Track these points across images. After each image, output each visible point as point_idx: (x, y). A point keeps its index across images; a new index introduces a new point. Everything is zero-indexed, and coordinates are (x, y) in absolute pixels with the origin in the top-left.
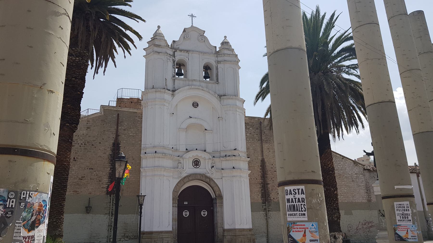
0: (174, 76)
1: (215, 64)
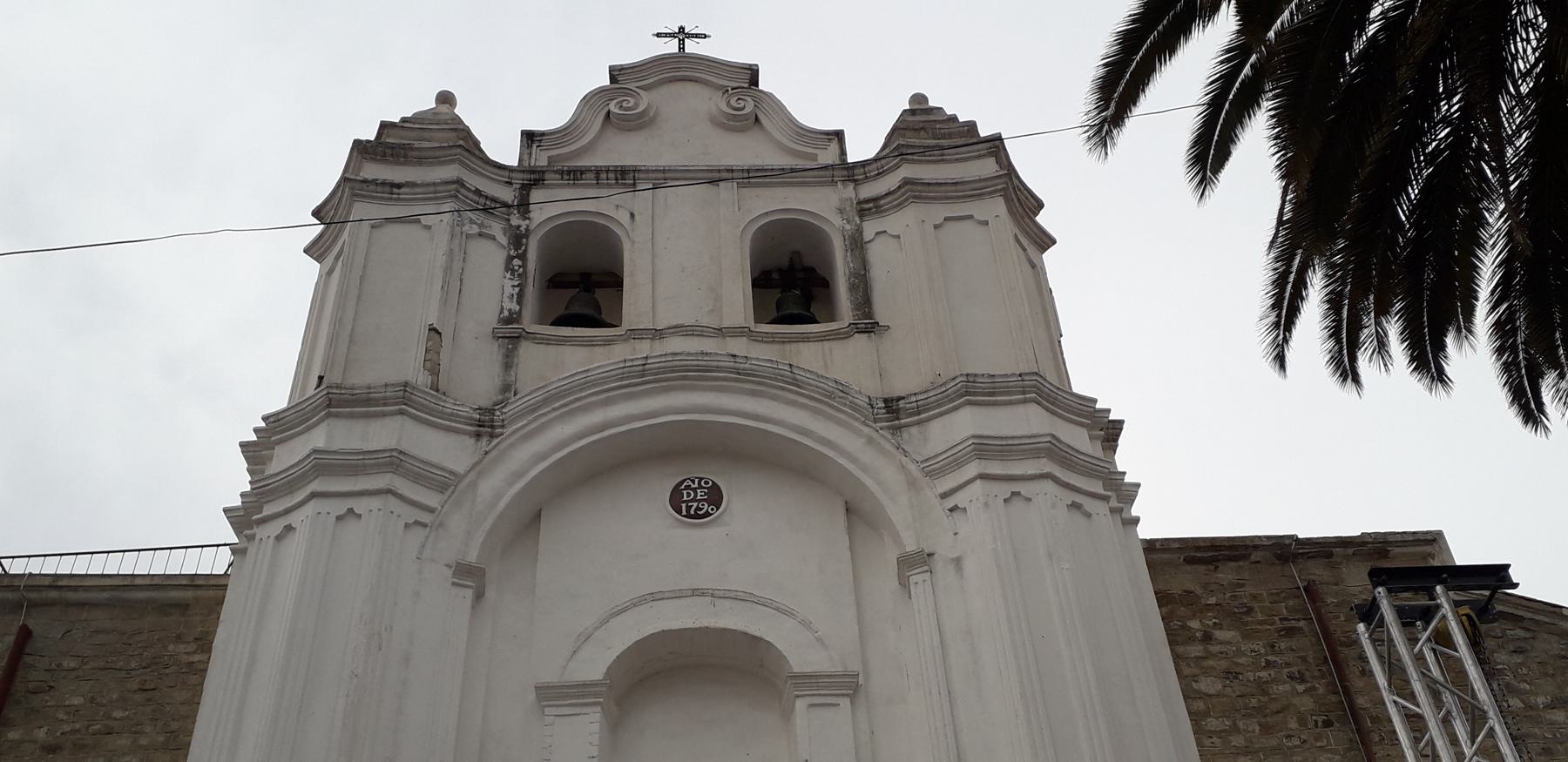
1: (837, 221)
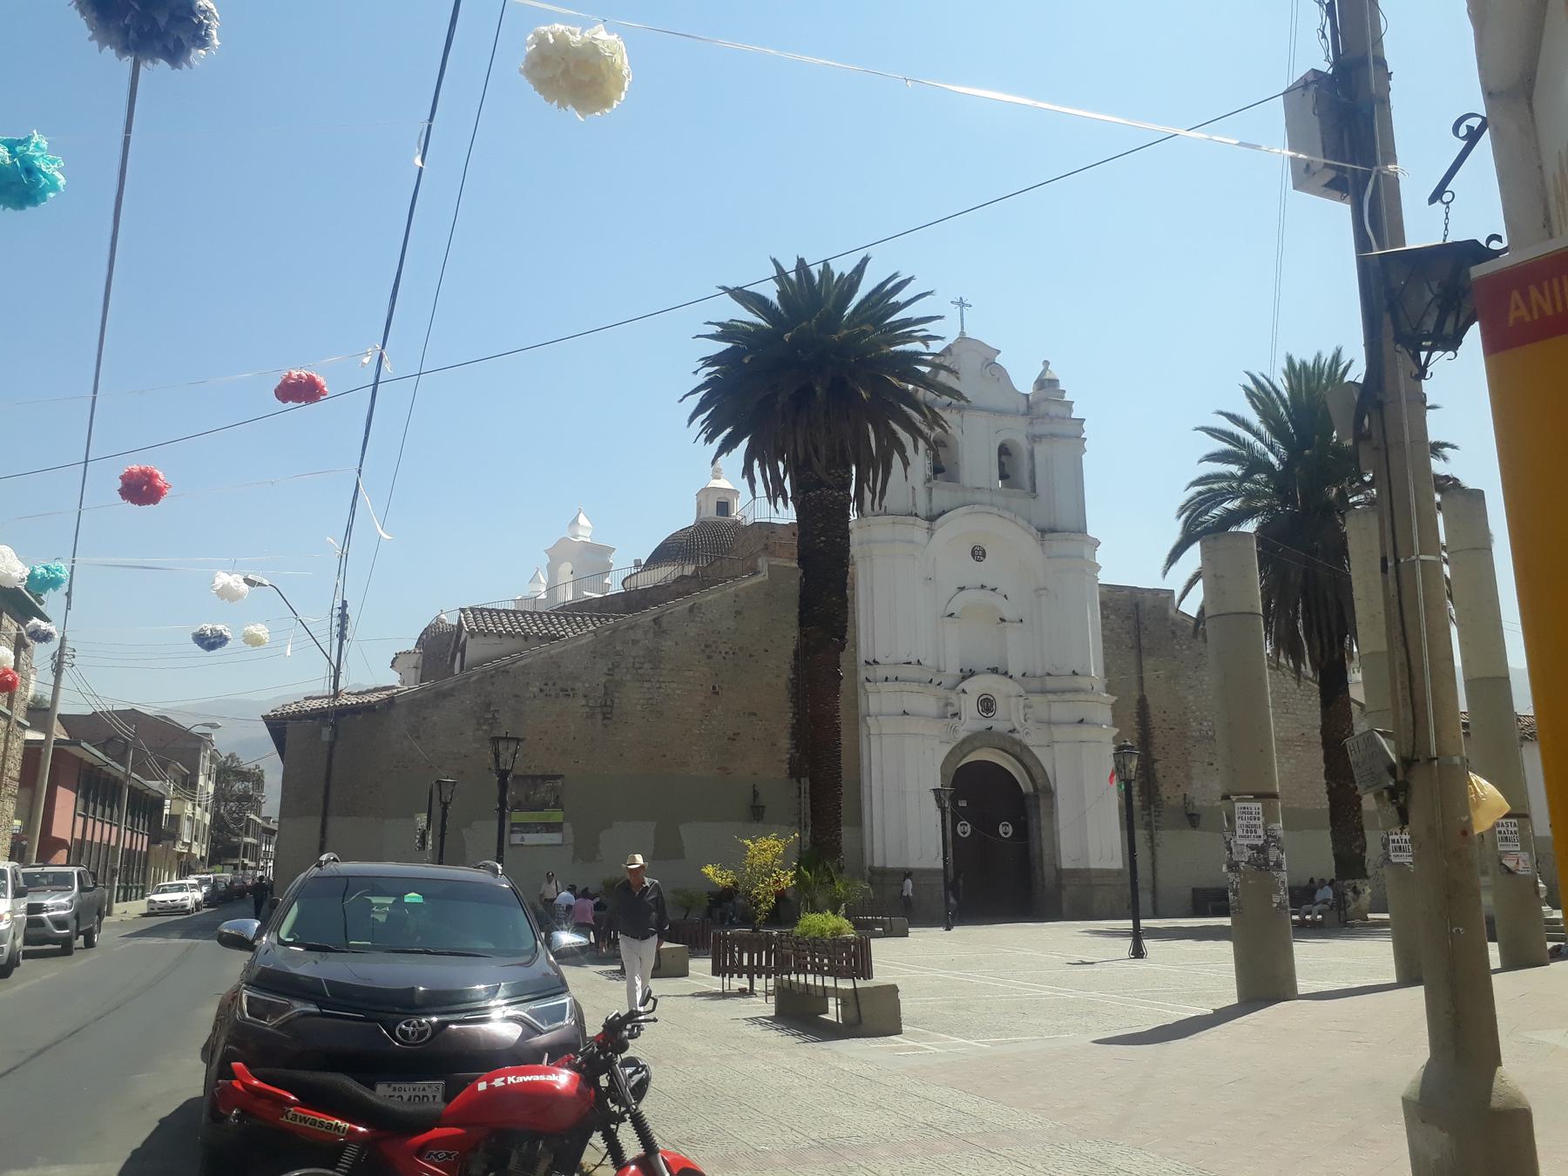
0: (929, 480)
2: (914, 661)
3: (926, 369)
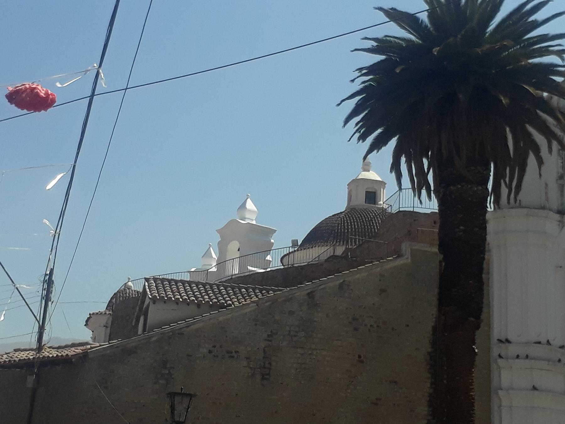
2: (544, 341)
3: (559, 79)
